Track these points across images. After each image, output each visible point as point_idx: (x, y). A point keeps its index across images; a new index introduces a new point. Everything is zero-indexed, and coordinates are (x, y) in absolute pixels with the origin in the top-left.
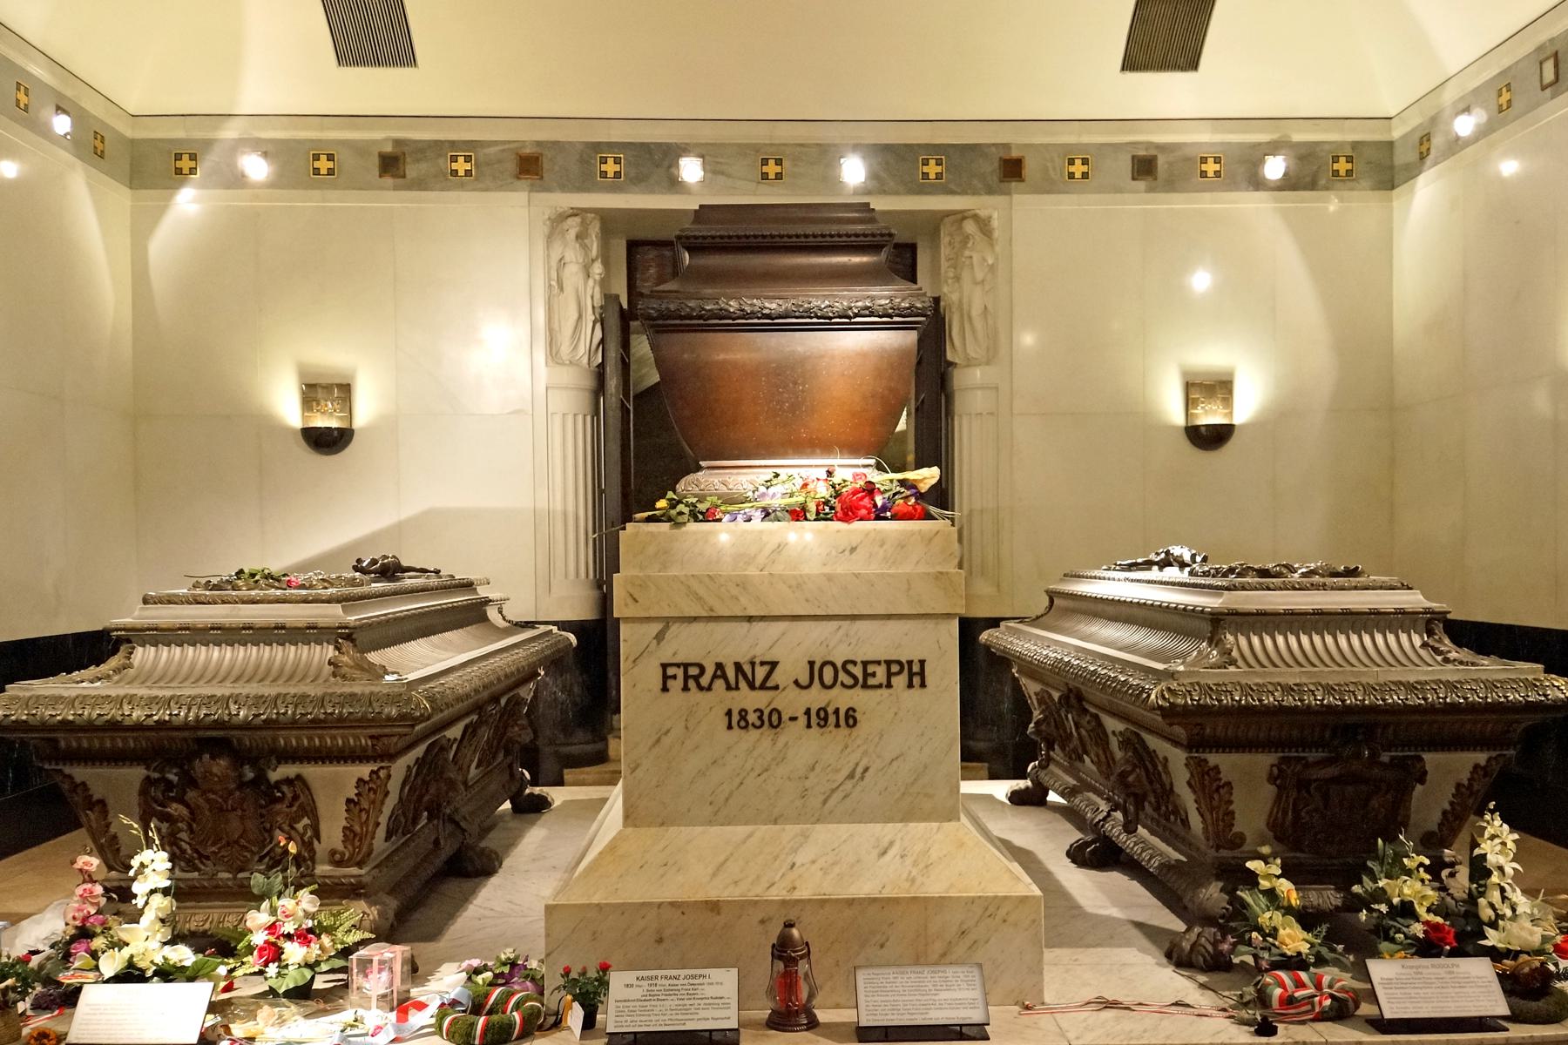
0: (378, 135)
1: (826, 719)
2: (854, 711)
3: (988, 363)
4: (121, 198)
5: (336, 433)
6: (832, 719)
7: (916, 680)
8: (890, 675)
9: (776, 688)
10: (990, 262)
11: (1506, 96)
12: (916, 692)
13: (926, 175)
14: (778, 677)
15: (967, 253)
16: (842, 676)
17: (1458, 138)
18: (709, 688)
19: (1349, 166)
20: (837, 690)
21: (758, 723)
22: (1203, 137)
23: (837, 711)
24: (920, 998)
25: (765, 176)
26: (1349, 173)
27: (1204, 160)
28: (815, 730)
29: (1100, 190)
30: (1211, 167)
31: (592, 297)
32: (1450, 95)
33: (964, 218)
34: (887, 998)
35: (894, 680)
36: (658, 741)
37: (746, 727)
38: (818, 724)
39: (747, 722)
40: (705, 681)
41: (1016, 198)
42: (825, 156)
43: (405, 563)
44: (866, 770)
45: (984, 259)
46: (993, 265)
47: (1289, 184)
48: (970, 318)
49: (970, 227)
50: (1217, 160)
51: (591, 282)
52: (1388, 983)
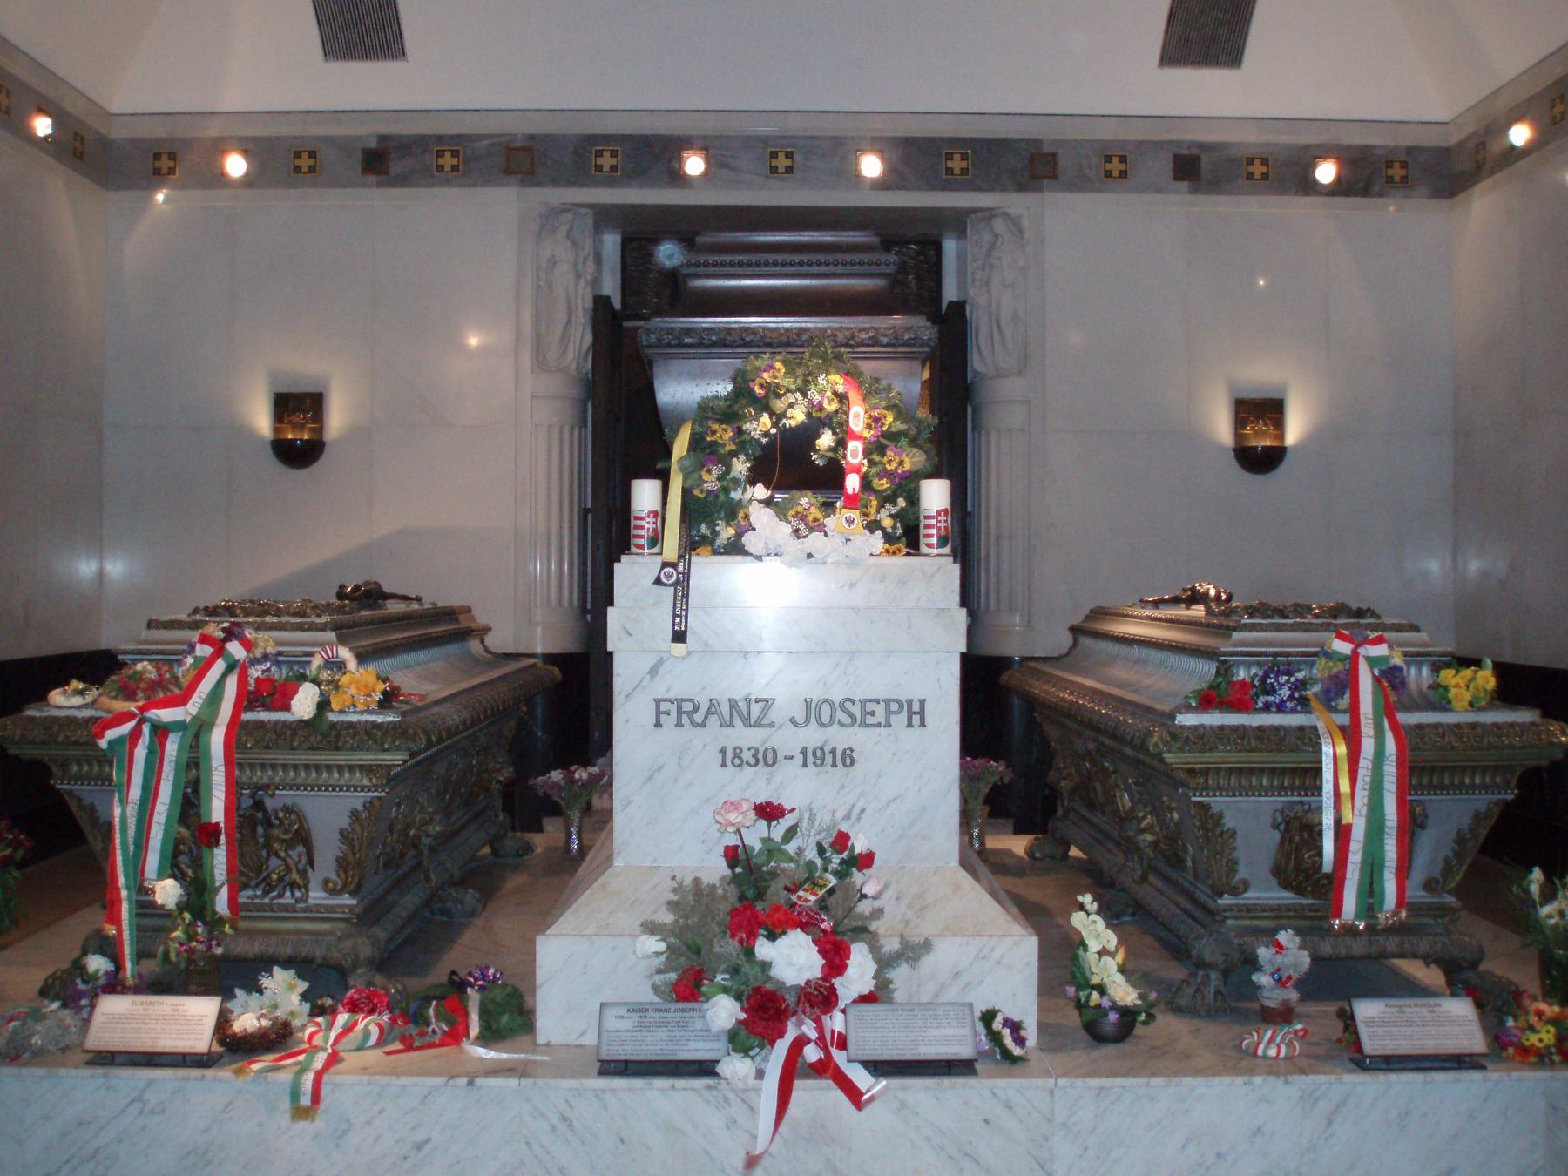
1: (823, 760)
2: (852, 751)
3: (1019, 373)
6: (829, 758)
7: (916, 719)
8: (888, 713)
9: (772, 725)
10: (1021, 263)
11: (1559, 108)
12: (917, 731)
14: (775, 715)
16: (840, 715)
17: (1513, 148)
18: (703, 725)
19: (1403, 172)
20: (836, 726)
21: (752, 761)
23: (833, 751)
24: (909, 1034)
25: (774, 170)
26: (1404, 179)
28: (811, 768)
29: (1143, 189)
30: (1258, 169)
31: (583, 298)
34: (876, 1034)
35: (893, 719)
36: (650, 778)
37: (740, 765)
38: (815, 763)
39: (741, 759)
40: (699, 717)
42: (840, 151)
43: (387, 589)
44: (863, 811)
47: (1340, 188)
49: (999, 225)
51: (582, 282)
52: (1370, 1021)
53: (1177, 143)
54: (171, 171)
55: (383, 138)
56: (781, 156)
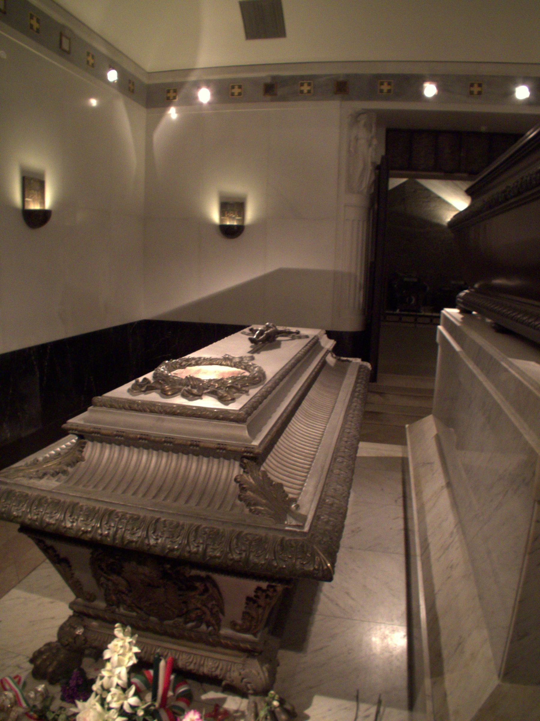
0: (263, 74)
4: (141, 112)
5: (235, 228)
25: (472, 93)
54: (175, 98)
55: (274, 78)
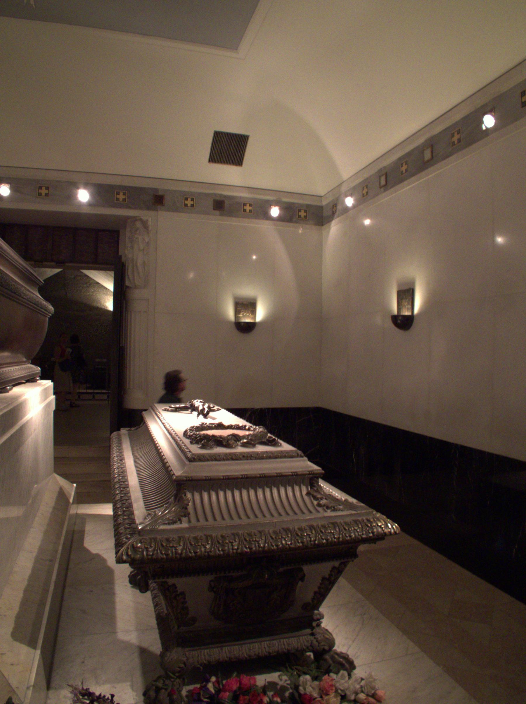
10: (147, 240)
13: (118, 199)
15: (136, 236)
22: (245, 195)
25: (40, 194)
26: (305, 217)
27: (245, 205)
32: (344, 188)
33: (137, 220)
41: (160, 213)
45: (144, 240)
46: (148, 243)
48: (136, 266)
49: (138, 224)
50: (251, 205)
53: (215, 195)
56: (44, 188)
